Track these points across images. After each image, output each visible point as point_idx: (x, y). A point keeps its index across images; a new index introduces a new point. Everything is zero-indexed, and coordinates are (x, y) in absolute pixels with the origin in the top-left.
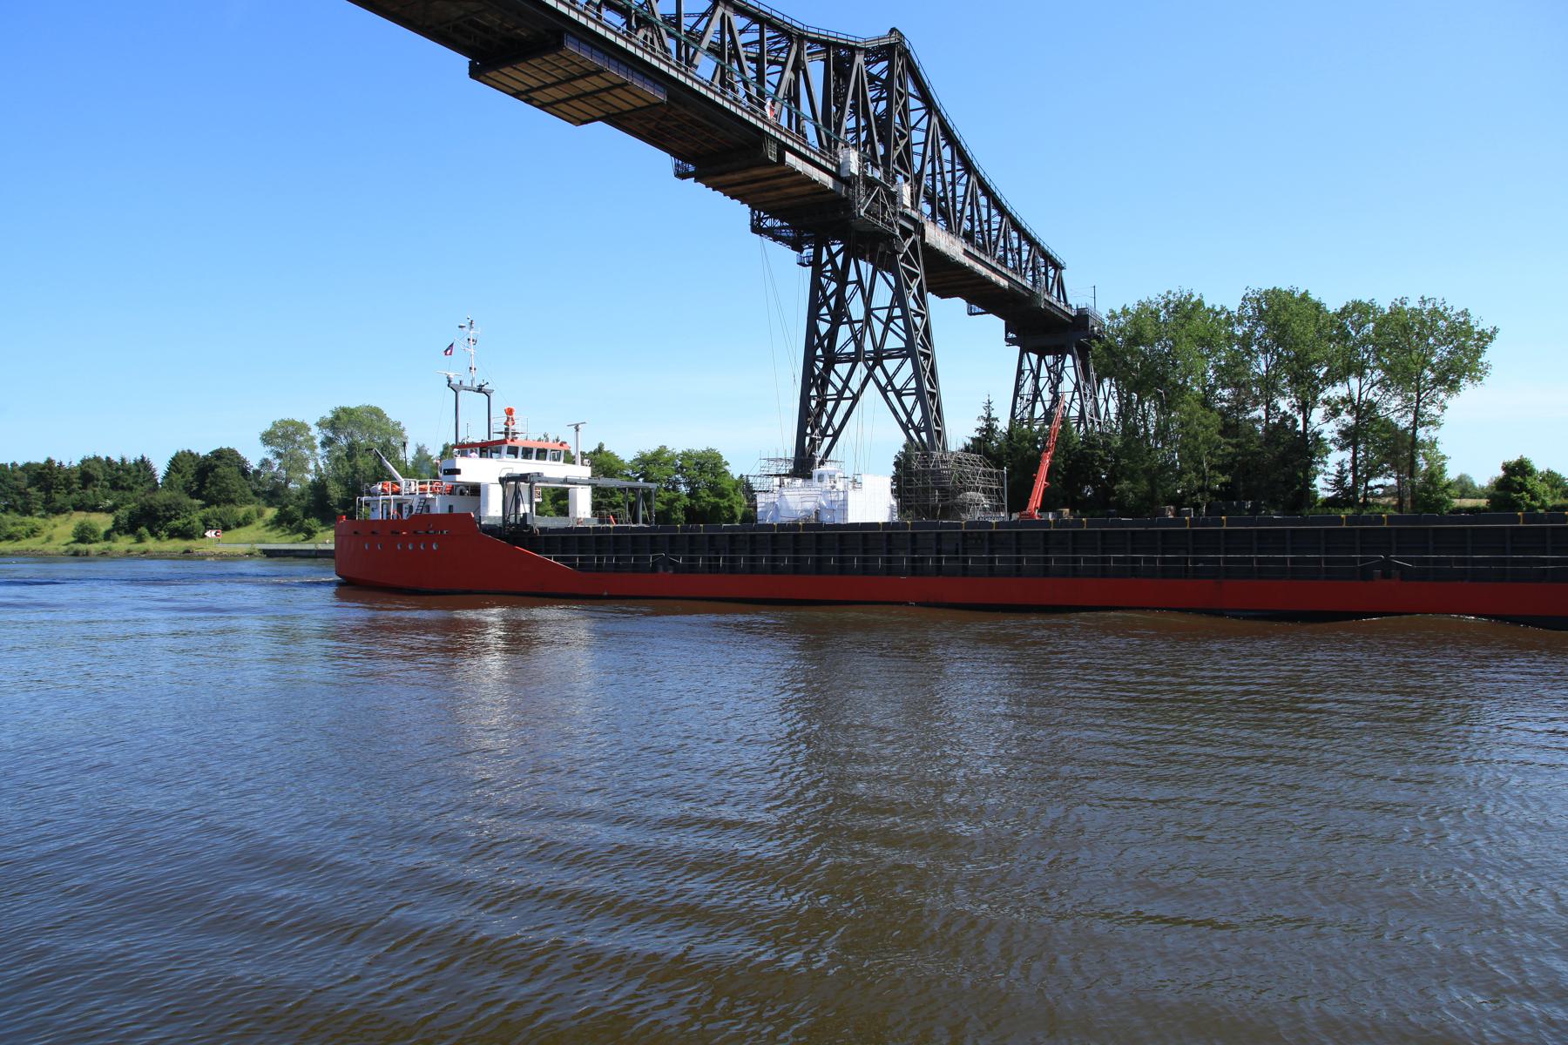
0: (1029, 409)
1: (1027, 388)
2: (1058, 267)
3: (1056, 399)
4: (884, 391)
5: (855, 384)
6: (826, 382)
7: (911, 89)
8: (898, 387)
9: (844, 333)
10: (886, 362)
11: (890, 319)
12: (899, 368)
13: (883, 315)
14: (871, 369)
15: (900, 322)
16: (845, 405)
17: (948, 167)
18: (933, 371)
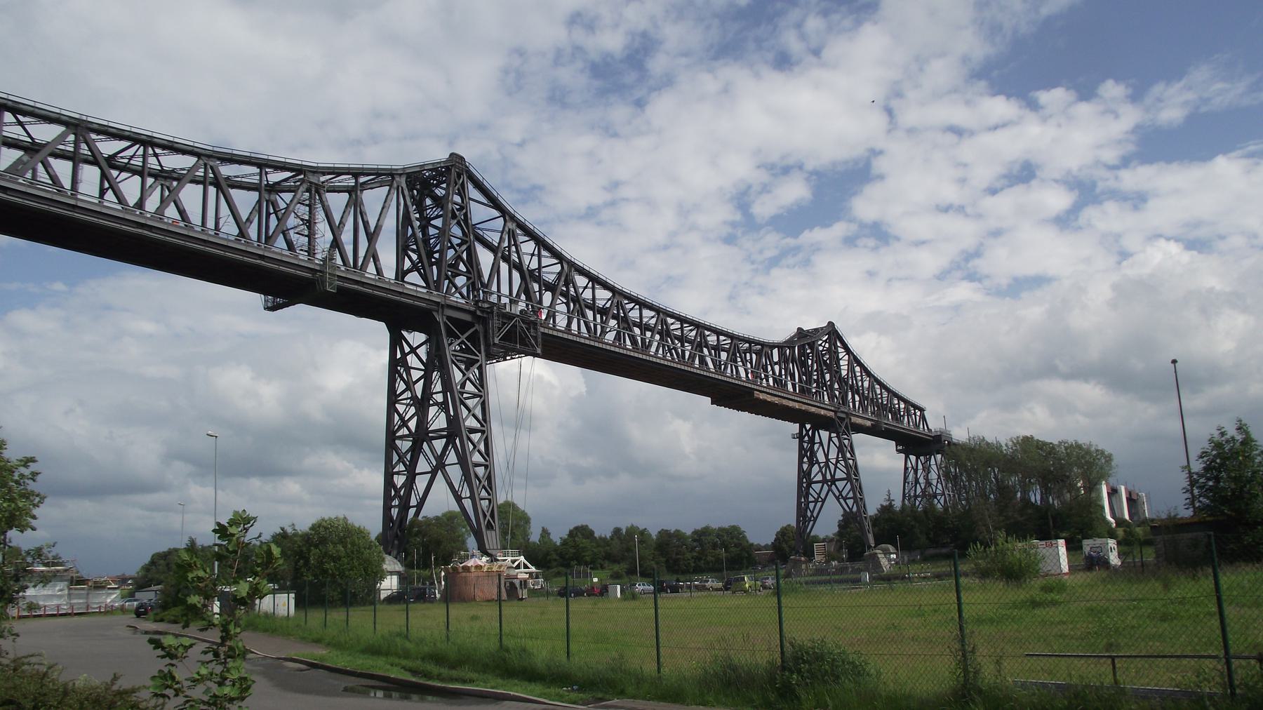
0: (913, 488)
1: (911, 477)
2: (922, 410)
3: (928, 483)
4: (838, 499)
5: (823, 496)
6: (808, 494)
7: (839, 344)
8: (844, 495)
9: (816, 468)
10: (837, 483)
11: (838, 461)
12: (848, 493)
13: (834, 461)
14: (830, 487)
15: (842, 463)
16: (819, 504)
17: (858, 374)
18: (860, 488)
